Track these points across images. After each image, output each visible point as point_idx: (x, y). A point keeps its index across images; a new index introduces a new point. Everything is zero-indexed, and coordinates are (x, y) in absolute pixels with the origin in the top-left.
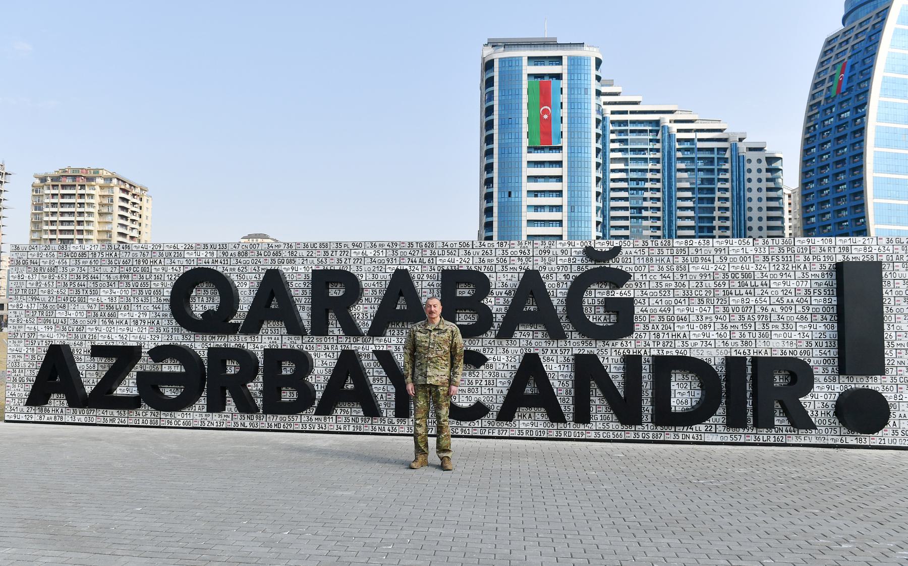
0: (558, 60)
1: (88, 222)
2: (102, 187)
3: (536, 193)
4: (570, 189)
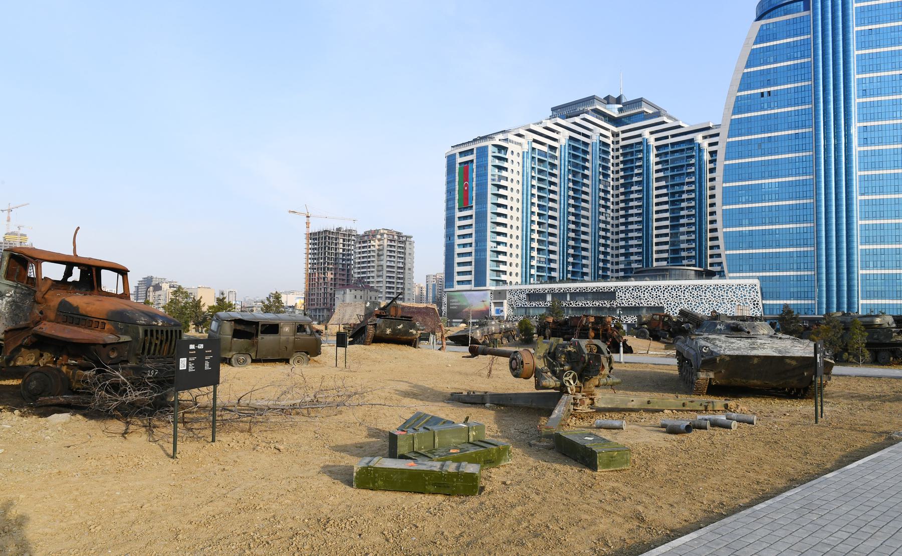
2: (379, 240)
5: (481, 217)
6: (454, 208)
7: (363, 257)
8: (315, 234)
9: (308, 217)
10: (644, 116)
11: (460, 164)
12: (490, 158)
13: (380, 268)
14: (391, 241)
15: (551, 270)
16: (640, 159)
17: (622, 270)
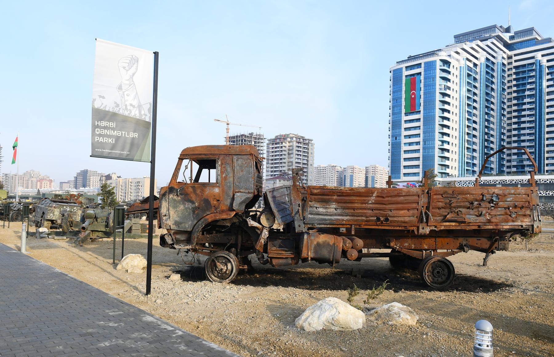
0: (419, 65)
1: (284, 158)
2: (289, 142)
3: (410, 136)
4: (424, 133)
5: (429, 120)
6: (401, 113)
7: (276, 156)
8: (234, 137)
9: (228, 124)
10: (535, 41)
11: (406, 76)
12: (438, 71)
13: (290, 164)
14: (298, 143)
15: (474, 165)
16: (533, 76)
17: (514, 166)
